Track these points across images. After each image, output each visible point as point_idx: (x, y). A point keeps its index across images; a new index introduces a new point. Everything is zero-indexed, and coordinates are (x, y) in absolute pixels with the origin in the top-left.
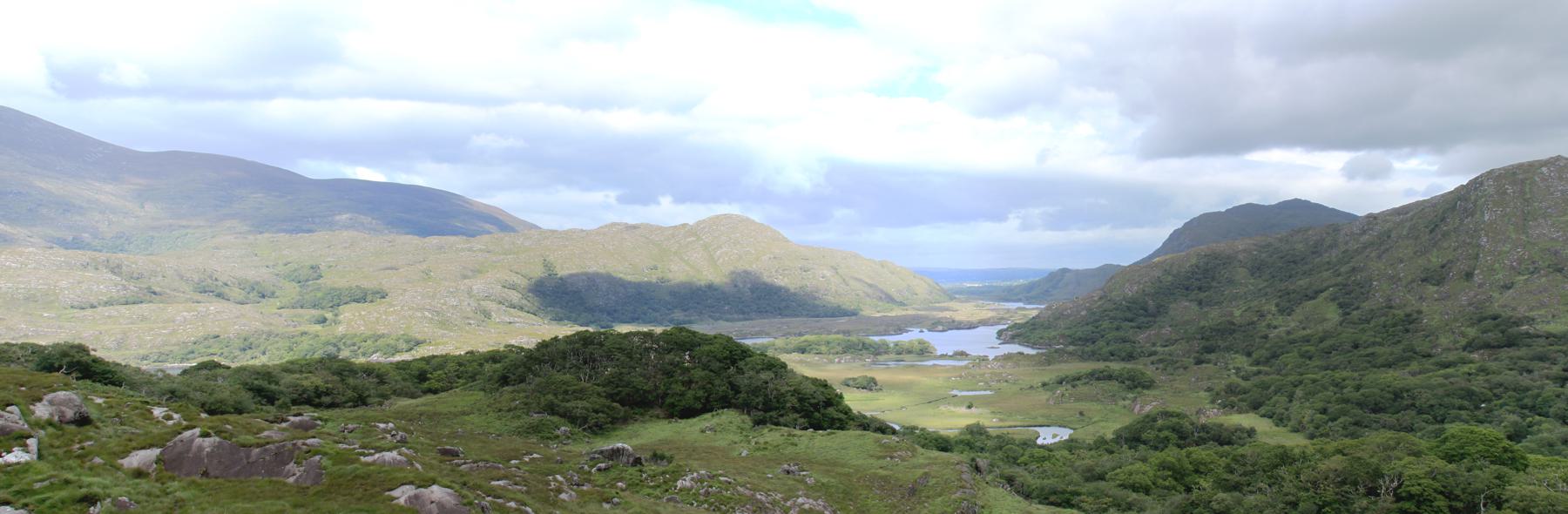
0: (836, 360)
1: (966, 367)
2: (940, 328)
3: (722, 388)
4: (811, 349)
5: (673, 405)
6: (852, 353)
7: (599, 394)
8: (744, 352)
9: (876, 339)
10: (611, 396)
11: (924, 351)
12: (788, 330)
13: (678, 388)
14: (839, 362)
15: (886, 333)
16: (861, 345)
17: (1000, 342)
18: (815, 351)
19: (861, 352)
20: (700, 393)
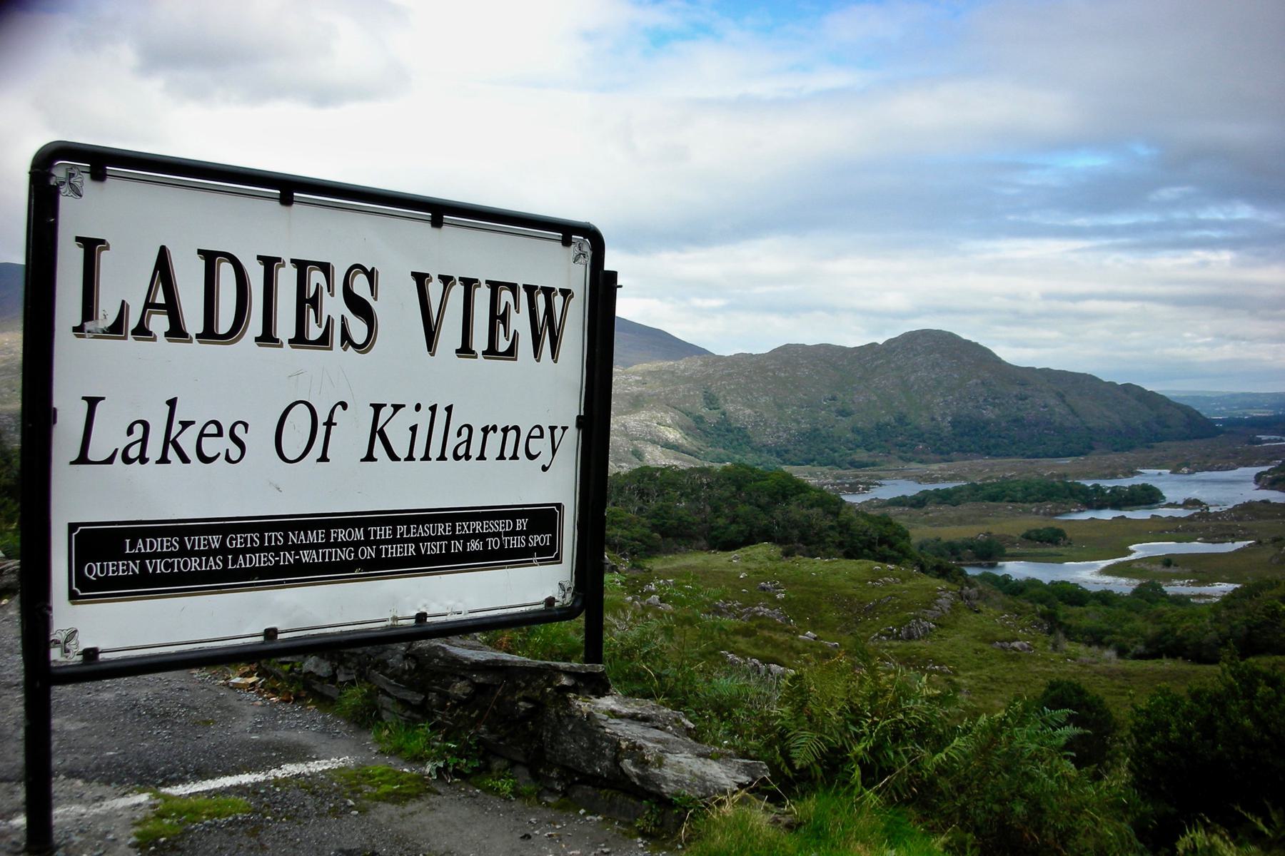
0: (1034, 510)
1: (1190, 518)
2: (1185, 470)
3: (763, 520)
4: (1004, 497)
5: (716, 538)
6: (1055, 501)
7: (643, 526)
8: (797, 487)
9: (1089, 484)
10: (655, 528)
11: (1149, 497)
12: (991, 474)
13: (721, 521)
14: (1037, 513)
15: (1113, 476)
16: (1067, 491)
17: (1257, 487)
18: (1008, 498)
19: (1066, 501)
20: (743, 527)
